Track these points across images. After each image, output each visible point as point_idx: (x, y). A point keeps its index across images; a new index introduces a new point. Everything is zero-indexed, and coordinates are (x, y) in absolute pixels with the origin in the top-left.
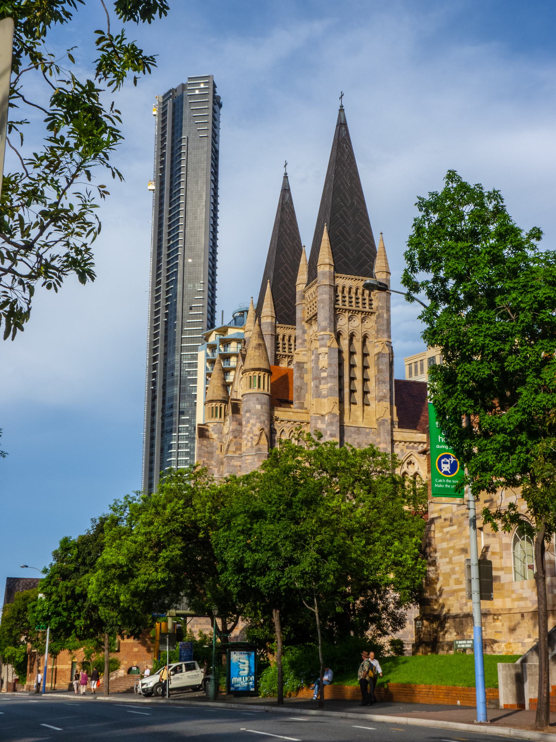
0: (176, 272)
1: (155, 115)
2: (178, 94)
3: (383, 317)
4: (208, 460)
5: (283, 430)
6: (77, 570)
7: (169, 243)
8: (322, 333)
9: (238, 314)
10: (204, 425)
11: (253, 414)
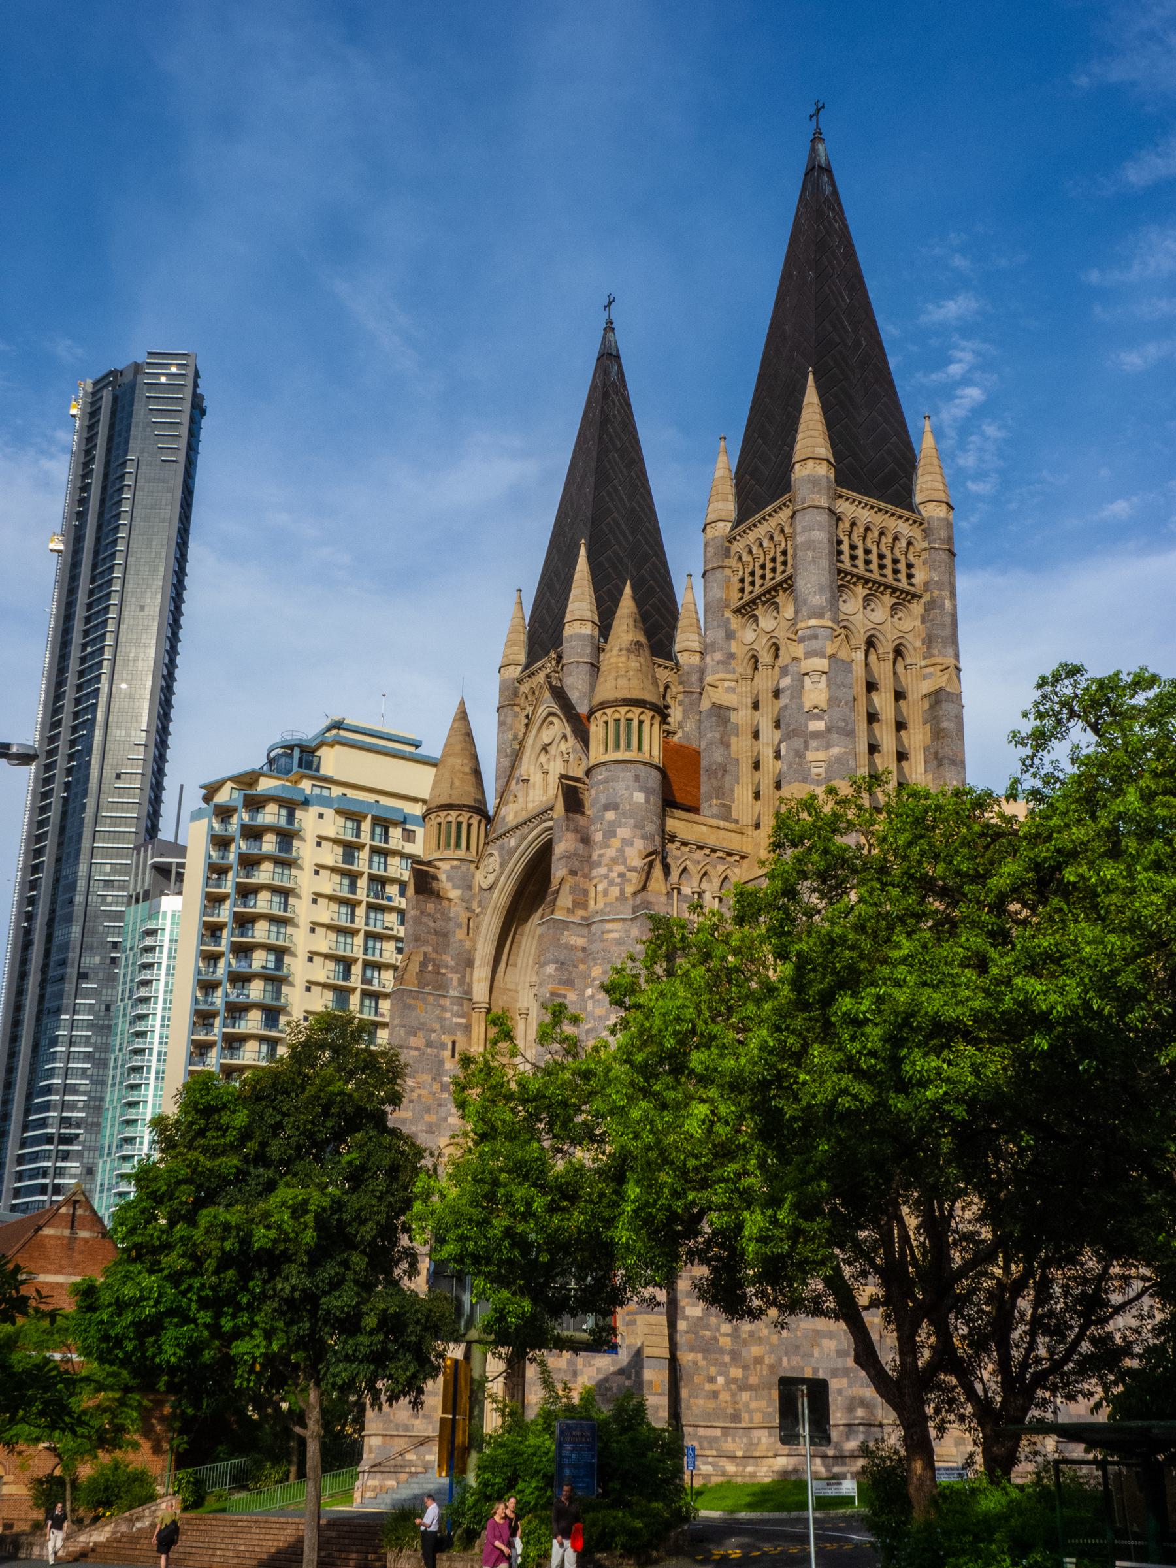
0: (95, 706)
1: (73, 416)
2: (127, 379)
3: (942, 607)
4: (435, 951)
5: (685, 869)
6: (241, 1175)
7: (84, 650)
8: (813, 622)
9: (280, 751)
10: (428, 864)
11: (624, 814)
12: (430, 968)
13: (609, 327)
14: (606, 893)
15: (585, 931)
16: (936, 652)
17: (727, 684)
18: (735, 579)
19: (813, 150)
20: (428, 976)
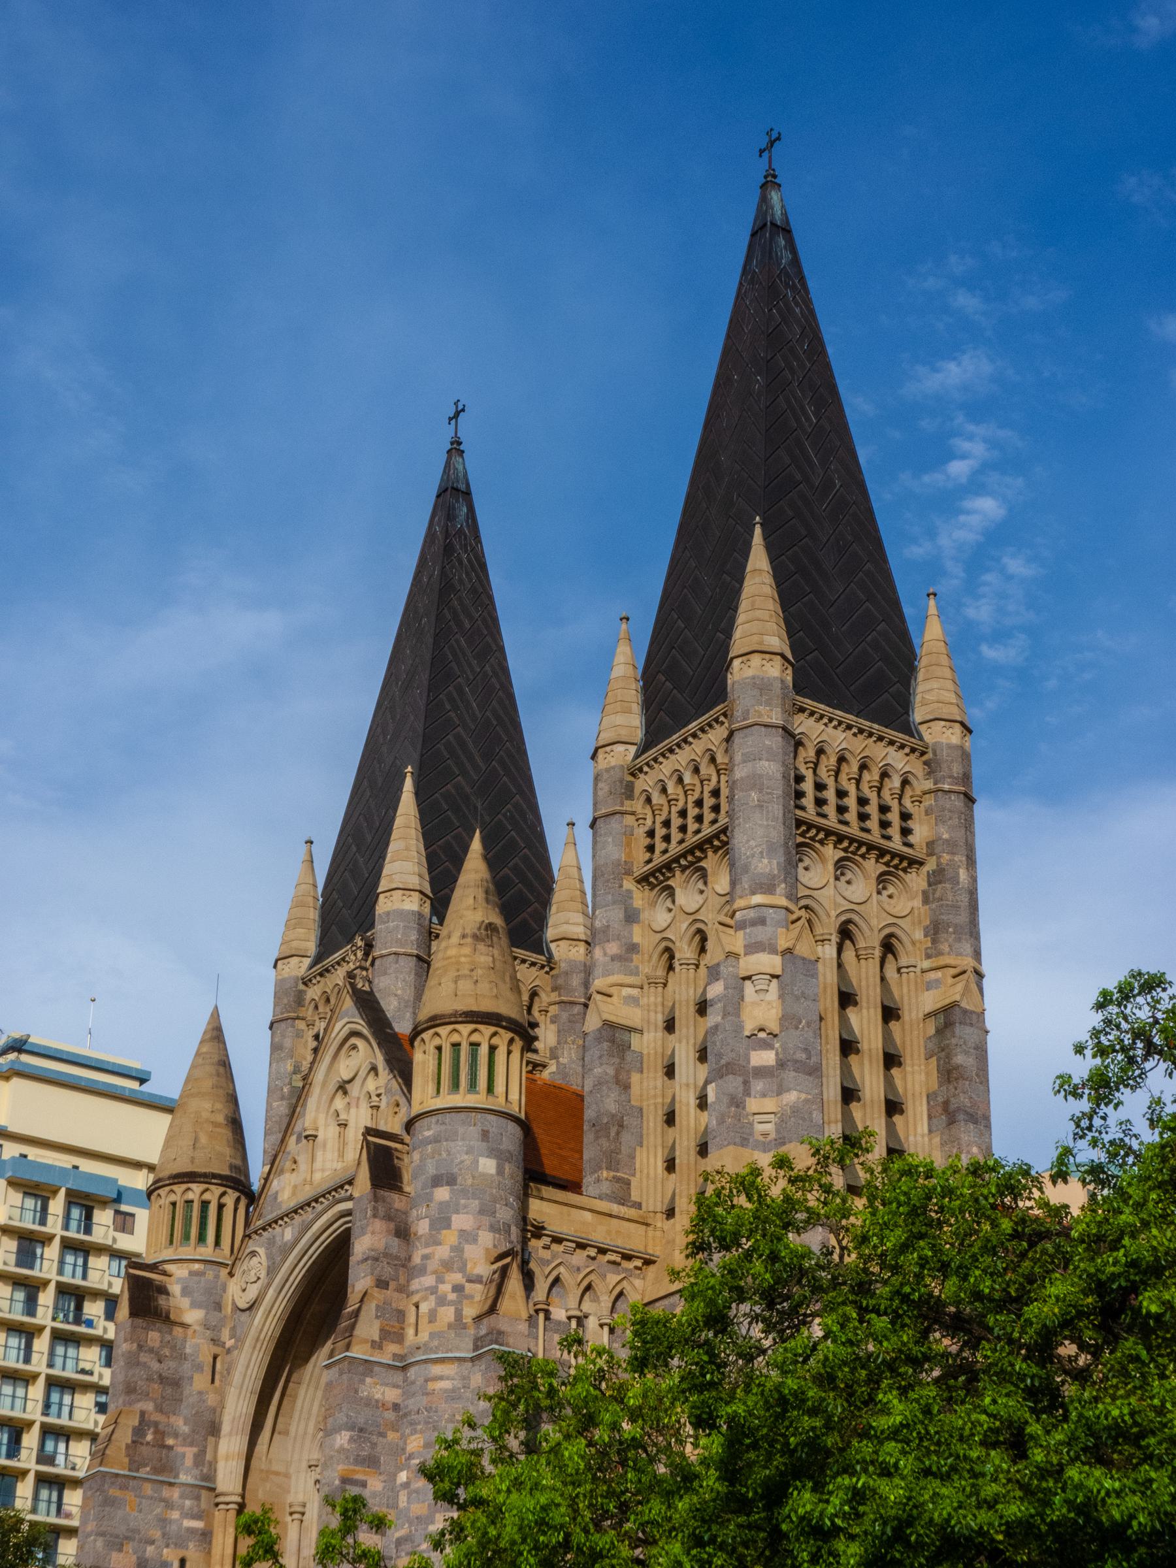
3: (955, 880)
4: (159, 1409)
5: (557, 1280)
8: (757, 899)
10: (153, 1267)
11: (464, 1192)
12: (149, 1437)
13: (456, 448)
14: (433, 1316)
15: (398, 1377)
16: (945, 947)
17: (626, 991)
18: (641, 832)
19: (764, 200)
20: (144, 1450)
